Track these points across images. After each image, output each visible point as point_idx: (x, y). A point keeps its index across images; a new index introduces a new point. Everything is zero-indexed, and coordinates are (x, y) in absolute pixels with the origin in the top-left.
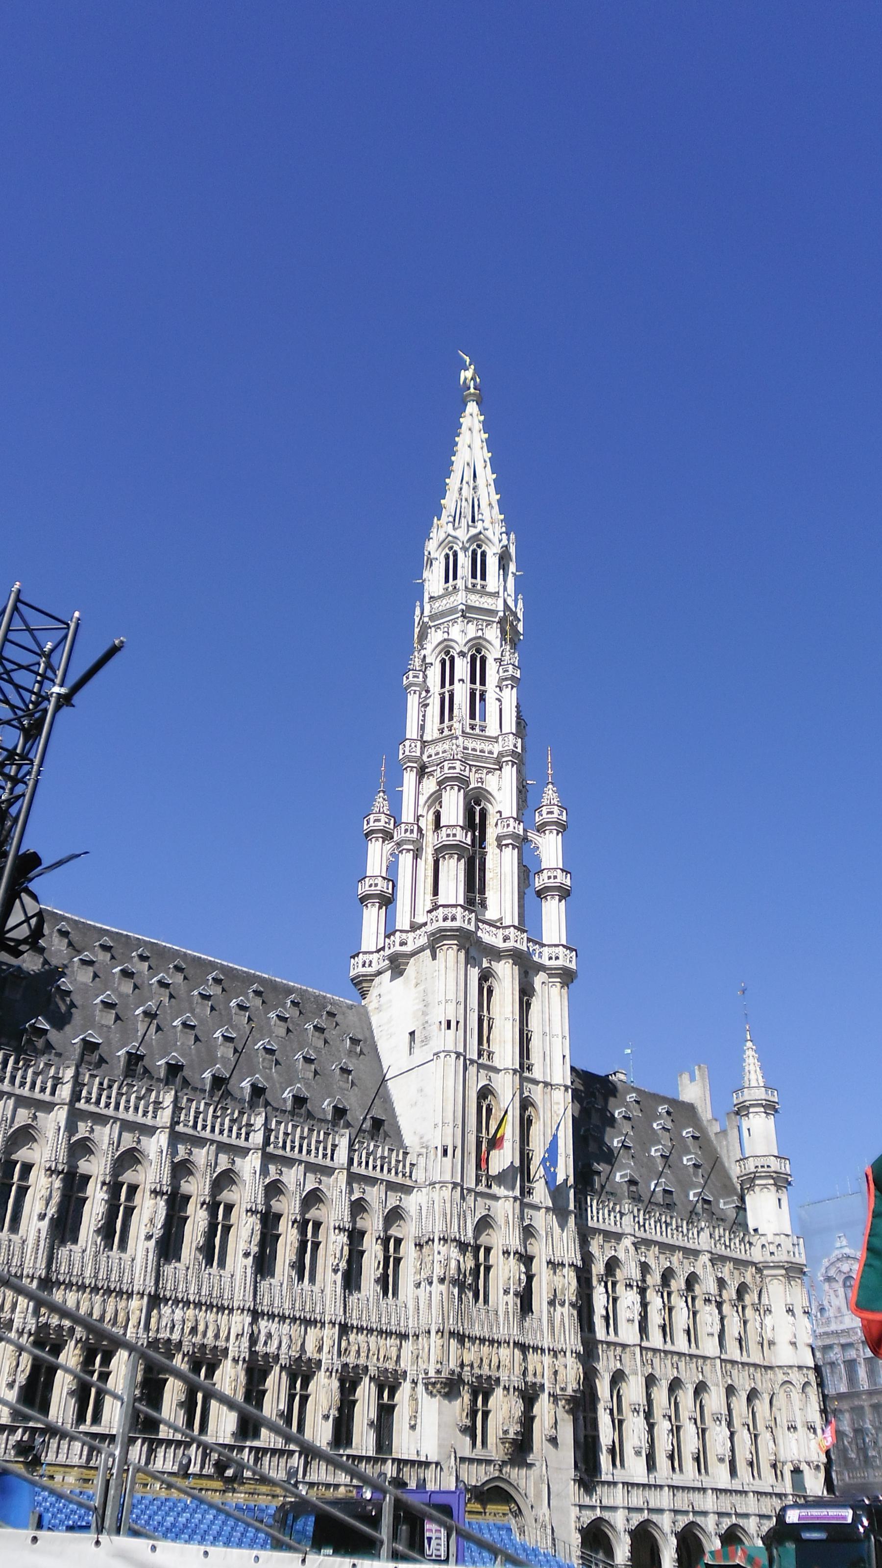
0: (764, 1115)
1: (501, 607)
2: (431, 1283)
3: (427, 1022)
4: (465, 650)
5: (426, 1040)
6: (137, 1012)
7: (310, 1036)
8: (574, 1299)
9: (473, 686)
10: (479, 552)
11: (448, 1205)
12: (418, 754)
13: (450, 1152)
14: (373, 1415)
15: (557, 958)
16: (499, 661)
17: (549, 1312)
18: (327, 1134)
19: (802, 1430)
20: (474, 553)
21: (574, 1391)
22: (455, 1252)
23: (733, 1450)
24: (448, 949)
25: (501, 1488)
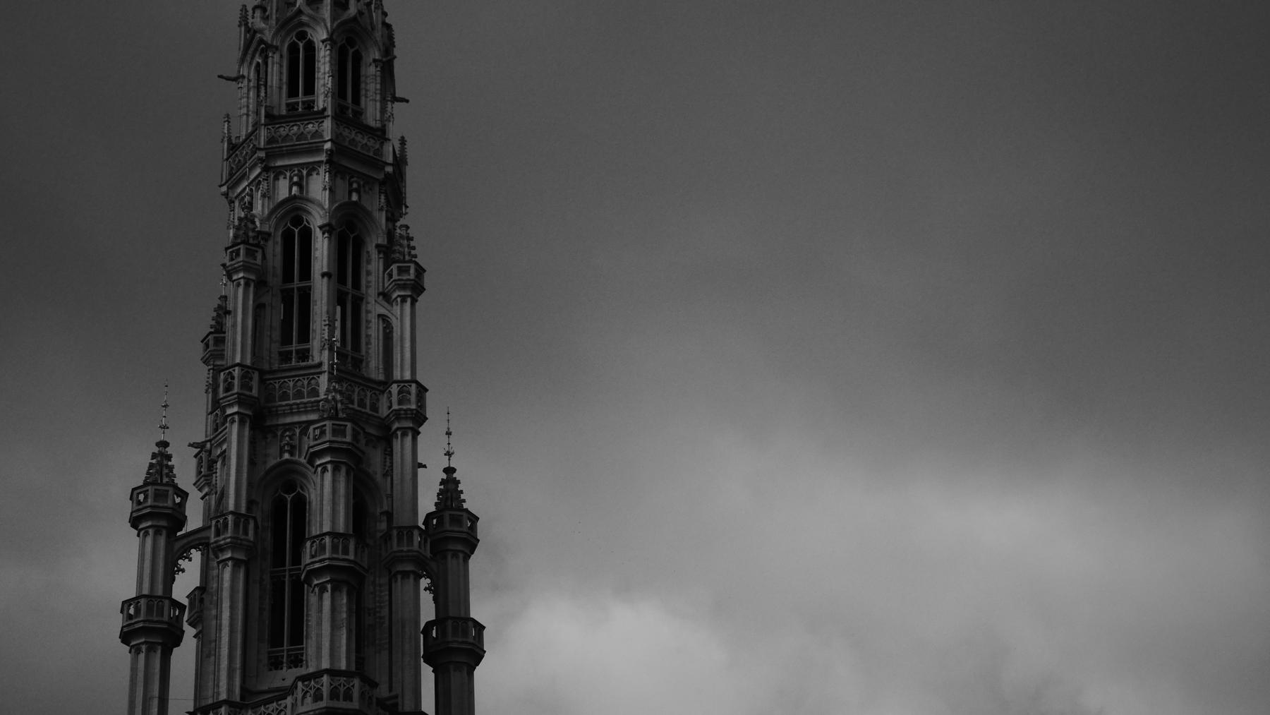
4: (334, 223)
10: (351, 51)
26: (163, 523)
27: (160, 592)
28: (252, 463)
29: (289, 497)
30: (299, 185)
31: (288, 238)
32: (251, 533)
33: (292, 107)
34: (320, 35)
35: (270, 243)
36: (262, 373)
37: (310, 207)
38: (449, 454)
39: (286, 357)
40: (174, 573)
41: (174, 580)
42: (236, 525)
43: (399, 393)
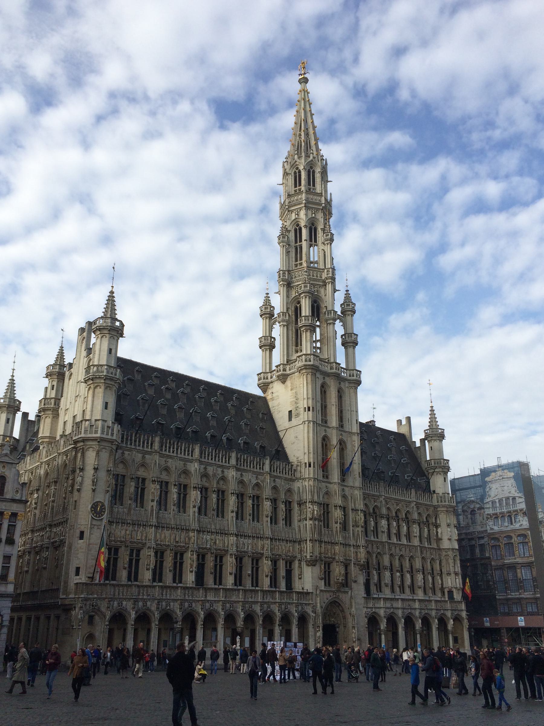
0: (438, 441)
1: (323, 201)
2: (306, 520)
3: (298, 407)
4: (307, 225)
5: (298, 415)
6: (175, 407)
7: (245, 413)
8: (363, 525)
9: (311, 243)
10: (311, 171)
11: (313, 488)
12: (287, 278)
13: (312, 465)
14: (284, 575)
15: (353, 376)
16: (323, 230)
17: (353, 530)
18: (260, 459)
19: (453, 575)
20: (309, 171)
21: (363, 562)
22: (316, 509)
23: (424, 583)
24: (307, 374)
25: (337, 602)
26: (268, 316)
27: (268, 335)
28: (288, 297)
29: (298, 305)
30: (298, 215)
31: (296, 230)
32: (287, 317)
33: (296, 191)
34: (301, 167)
35: (291, 232)
36: (289, 271)
37: (300, 220)
38: (347, 286)
39: (296, 265)
40: (272, 329)
41: (272, 331)
42: (283, 315)
43: (327, 272)
